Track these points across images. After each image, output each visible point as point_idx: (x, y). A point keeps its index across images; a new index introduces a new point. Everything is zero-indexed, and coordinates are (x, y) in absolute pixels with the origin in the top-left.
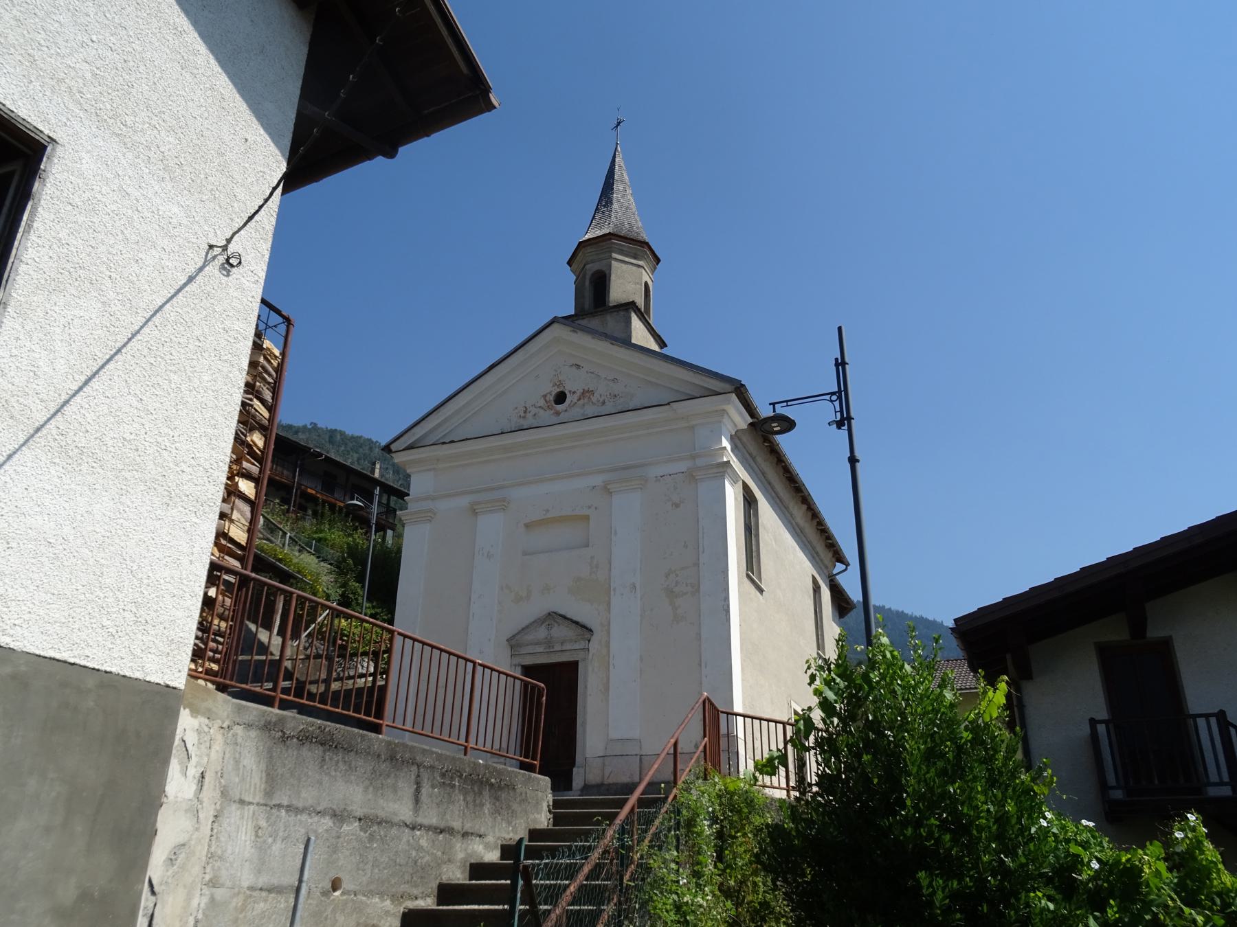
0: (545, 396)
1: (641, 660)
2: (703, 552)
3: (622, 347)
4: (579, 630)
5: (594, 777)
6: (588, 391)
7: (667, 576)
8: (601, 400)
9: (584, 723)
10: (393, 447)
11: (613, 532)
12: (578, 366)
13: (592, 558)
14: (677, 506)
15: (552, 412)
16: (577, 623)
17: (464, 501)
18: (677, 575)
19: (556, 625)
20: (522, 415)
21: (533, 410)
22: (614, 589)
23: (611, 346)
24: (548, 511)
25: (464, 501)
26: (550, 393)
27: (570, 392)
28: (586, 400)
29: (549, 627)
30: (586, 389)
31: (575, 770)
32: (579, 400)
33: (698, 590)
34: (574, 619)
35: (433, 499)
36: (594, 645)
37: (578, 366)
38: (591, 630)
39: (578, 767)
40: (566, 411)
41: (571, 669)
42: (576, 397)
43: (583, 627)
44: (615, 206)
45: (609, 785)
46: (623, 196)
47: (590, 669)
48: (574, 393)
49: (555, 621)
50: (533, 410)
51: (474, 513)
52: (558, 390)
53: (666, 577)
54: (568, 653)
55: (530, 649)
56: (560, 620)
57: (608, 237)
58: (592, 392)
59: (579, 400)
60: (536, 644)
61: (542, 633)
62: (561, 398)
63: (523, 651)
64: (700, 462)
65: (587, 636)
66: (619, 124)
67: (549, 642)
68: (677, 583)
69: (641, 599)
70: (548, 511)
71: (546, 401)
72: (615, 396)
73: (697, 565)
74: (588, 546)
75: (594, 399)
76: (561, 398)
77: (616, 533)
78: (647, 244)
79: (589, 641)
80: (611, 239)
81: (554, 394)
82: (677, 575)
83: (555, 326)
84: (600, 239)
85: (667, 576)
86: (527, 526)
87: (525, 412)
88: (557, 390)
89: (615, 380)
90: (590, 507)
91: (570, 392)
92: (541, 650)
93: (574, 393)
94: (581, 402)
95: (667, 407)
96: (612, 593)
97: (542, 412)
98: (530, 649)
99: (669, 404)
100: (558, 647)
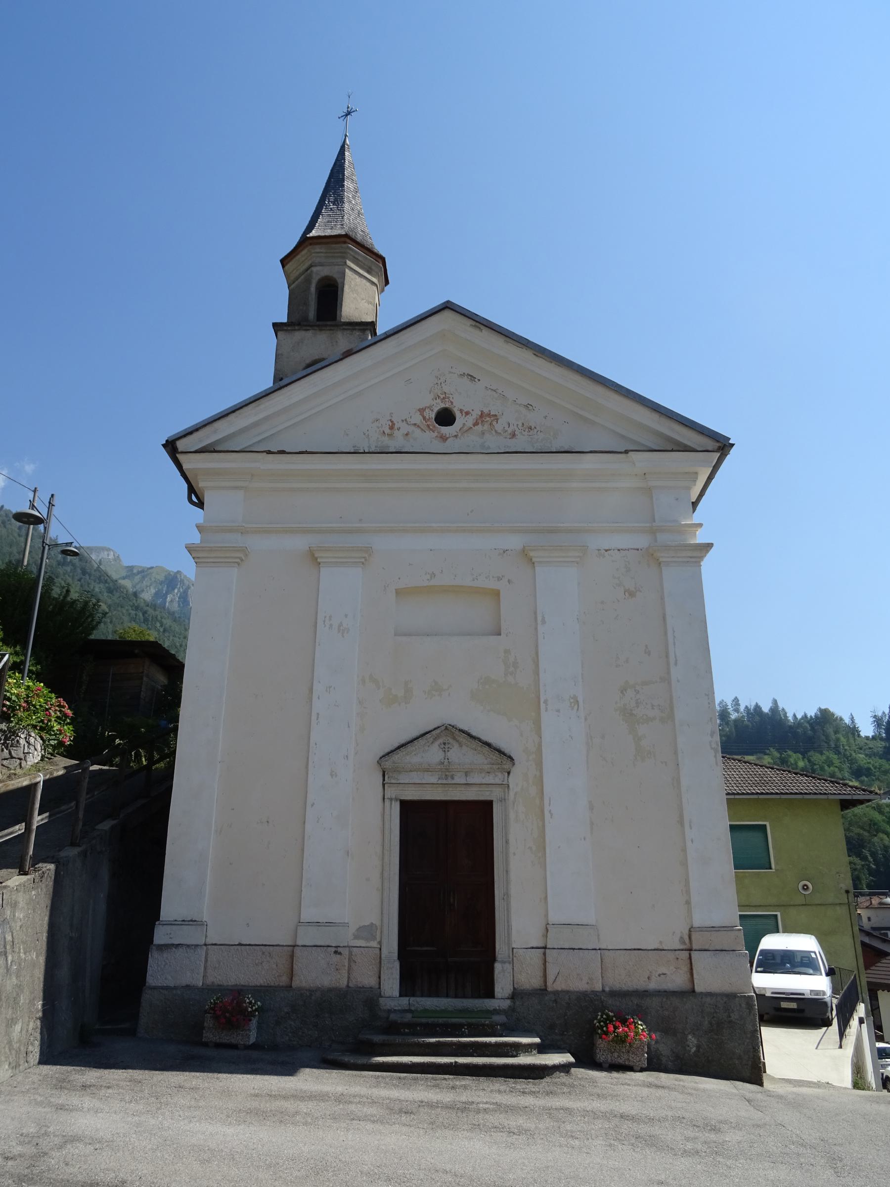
0: (422, 411)
1: (591, 808)
2: (676, 664)
3: (551, 362)
4: (495, 756)
5: (529, 979)
6: (489, 415)
7: (623, 691)
8: (510, 430)
9: (507, 895)
10: (181, 445)
11: (539, 618)
12: (472, 378)
13: (507, 652)
14: (632, 594)
15: (436, 434)
16: (488, 745)
17: (300, 543)
18: (638, 692)
19: (456, 745)
20: (387, 431)
21: (405, 428)
22: (546, 702)
23: (534, 356)
24: (433, 575)
25: (300, 543)
26: (430, 408)
27: (461, 411)
28: (486, 427)
29: (445, 747)
30: (486, 411)
31: (498, 967)
32: (476, 424)
33: (671, 716)
34: (484, 738)
35: (243, 532)
36: (516, 780)
37: (472, 378)
38: (510, 758)
39: (503, 962)
40: (456, 436)
41: (484, 809)
42: (470, 421)
43: (500, 752)
44: (346, 206)
45: (556, 993)
46: (354, 197)
47: (512, 816)
48: (467, 413)
49: (454, 739)
50: (405, 428)
51: (313, 558)
52: (443, 406)
53: (622, 692)
54: (475, 789)
55: (415, 777)
56: (462, 738)
57: (343, 239)
58: (496, 418)
59: (476, 424)
60: (427, 770)
61: (433, 754)
62: (445, 418)
63: (404, 778)
64: (662, 538)
65: (507, 765)
66: (349, 113)
67: (446, 770)
68: (638, 704)
69: (586, 719)
70: (433, 575)
71: (424, 418)
72: (530, 428)
73: (666, 679)
74: (500, 634)
75: (498, 427)
76: (445, 418)
77: (544, 622)
78: (383, 260)
79: (509, 773)
80: (345, 242)
81: (436, 409)
82: (638, 692)
83: (447, 314)
84: (334, 240)
85: (623, 691)
86: (398, 592)
87: (392, 428)
88: (439, 405)
89: (527, 406)
90: (499, 579)
91: (461, 411)
92: (434, 780)
93: (467, 413)
94: (479, 428)
95: (623, 456)
96: (543, 706)
97: (418, 432)
98: (415, 777)
99: (626, 452)
100: (459, 779)
